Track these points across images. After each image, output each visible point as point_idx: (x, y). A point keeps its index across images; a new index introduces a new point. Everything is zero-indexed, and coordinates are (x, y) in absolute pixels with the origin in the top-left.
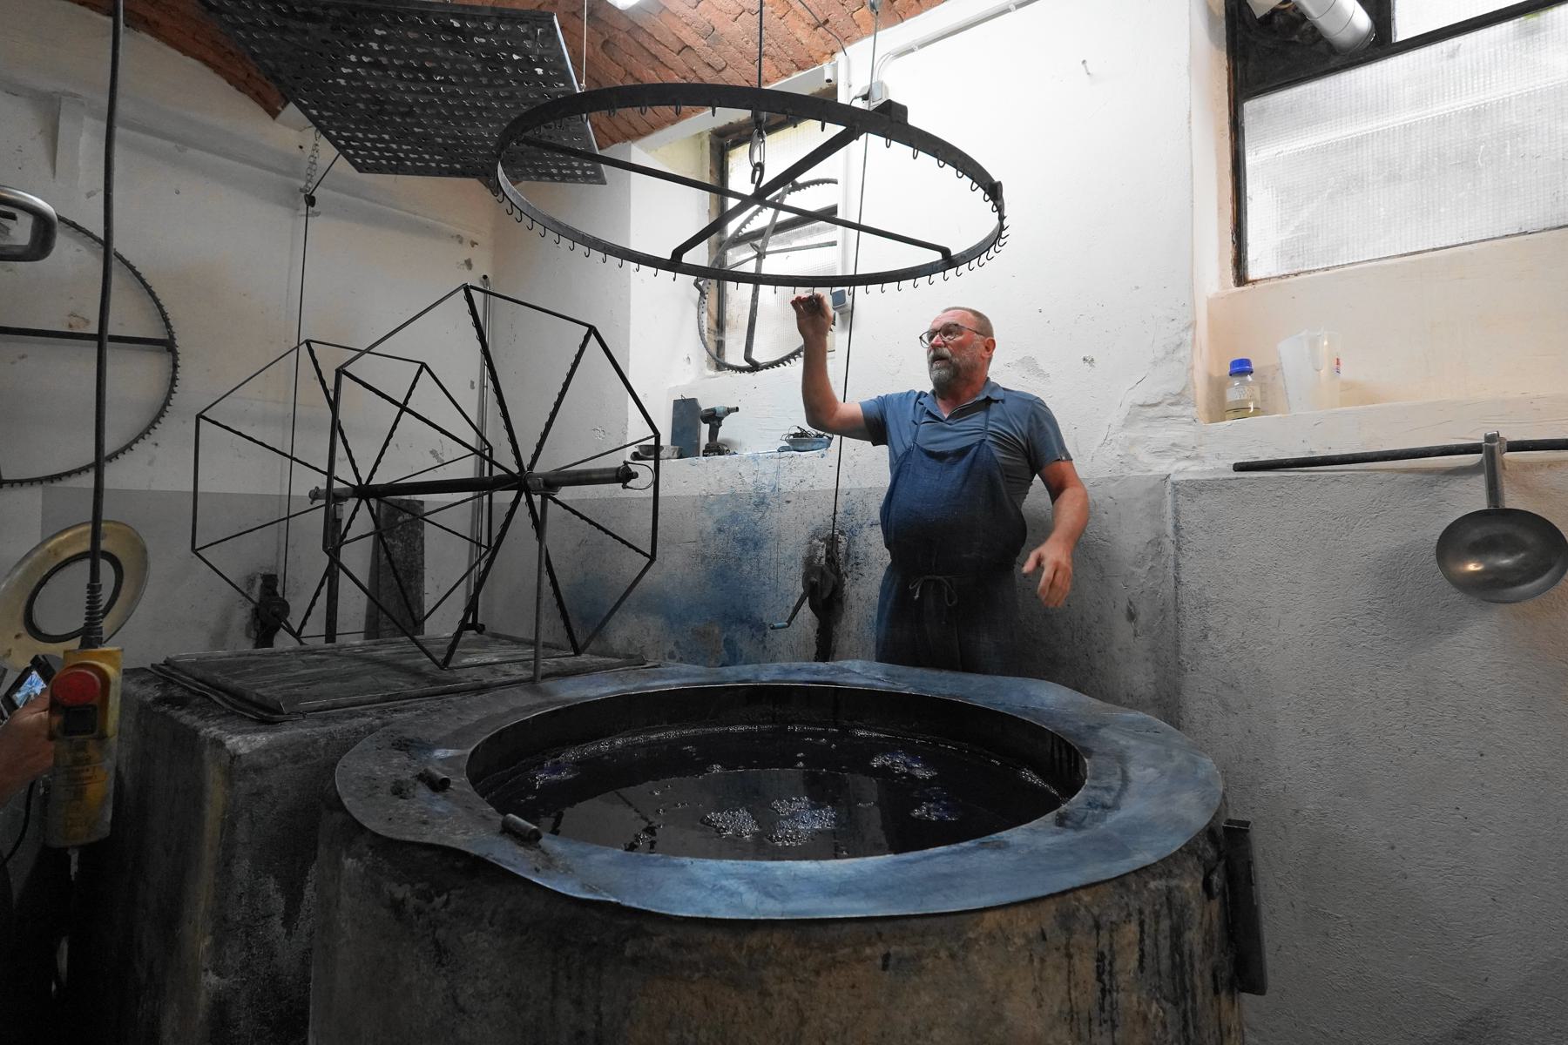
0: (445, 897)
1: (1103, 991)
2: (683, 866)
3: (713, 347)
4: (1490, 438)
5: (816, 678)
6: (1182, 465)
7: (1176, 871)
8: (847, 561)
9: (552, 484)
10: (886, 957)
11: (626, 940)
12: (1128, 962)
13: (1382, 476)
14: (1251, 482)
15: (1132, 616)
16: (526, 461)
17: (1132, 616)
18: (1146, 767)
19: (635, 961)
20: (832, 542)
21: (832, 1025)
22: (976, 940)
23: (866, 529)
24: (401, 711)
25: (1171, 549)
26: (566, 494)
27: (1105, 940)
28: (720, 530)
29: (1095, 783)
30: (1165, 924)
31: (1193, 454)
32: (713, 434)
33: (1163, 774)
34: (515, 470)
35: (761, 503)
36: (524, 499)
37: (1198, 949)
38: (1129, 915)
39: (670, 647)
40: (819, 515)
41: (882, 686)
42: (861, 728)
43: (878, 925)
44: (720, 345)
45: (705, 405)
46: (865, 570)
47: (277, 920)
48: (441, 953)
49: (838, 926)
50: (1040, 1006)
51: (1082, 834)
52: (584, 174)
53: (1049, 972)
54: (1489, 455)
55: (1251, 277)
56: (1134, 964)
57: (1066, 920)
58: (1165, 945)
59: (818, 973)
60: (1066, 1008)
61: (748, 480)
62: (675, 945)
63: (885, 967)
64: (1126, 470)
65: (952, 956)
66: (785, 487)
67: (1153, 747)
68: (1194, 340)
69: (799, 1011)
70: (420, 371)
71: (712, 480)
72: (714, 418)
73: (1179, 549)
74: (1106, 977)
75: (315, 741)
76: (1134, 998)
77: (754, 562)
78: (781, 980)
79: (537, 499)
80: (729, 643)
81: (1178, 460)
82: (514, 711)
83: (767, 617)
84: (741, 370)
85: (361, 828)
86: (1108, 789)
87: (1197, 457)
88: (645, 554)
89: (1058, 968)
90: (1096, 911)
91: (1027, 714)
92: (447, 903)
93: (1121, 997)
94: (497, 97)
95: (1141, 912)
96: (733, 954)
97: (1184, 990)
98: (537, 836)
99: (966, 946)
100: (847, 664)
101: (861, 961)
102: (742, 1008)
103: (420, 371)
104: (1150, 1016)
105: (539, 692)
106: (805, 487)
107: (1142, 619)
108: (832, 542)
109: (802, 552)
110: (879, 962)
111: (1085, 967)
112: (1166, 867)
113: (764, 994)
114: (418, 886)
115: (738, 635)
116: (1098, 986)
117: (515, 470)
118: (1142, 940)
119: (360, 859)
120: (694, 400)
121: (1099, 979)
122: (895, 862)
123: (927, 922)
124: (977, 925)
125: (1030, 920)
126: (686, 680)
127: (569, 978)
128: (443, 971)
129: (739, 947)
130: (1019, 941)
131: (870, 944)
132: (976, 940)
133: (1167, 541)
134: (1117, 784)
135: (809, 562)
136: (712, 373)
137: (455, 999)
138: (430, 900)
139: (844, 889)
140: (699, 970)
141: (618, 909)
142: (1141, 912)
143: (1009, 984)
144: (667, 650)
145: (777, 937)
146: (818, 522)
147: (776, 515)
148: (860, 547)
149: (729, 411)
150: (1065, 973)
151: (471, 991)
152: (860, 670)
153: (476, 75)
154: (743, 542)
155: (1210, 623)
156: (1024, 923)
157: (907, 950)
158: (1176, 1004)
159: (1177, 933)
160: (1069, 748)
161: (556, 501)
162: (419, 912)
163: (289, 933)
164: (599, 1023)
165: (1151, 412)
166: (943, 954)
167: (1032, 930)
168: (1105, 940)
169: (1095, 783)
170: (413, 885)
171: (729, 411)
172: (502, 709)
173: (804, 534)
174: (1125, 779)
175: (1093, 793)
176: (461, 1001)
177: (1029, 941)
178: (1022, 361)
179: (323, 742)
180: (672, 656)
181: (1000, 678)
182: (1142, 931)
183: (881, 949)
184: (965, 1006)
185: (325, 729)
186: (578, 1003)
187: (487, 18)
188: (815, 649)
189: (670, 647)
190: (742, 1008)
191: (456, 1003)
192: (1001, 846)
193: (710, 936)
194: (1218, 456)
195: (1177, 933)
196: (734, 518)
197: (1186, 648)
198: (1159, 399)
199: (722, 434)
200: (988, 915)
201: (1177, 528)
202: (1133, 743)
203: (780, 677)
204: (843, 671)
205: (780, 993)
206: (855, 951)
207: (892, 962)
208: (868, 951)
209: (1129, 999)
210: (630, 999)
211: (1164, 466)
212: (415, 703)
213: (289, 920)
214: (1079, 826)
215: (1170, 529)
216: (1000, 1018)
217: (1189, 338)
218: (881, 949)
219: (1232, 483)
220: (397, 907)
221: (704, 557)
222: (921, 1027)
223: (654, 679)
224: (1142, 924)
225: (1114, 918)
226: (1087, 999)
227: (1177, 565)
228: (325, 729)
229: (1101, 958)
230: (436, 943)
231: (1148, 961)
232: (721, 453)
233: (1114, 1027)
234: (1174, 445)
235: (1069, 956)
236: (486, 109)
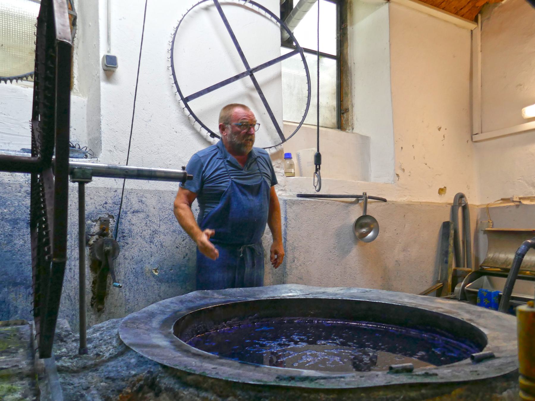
4: (365, 194)
13: (338, 203)
14: (308, 202)
23: (130, 215)
31: (283, 189)
46: (130, 240)
54: (362, 199)
55: (188, 103)
155: (295, 255)
194: (290, 191)
219: (302, 202)
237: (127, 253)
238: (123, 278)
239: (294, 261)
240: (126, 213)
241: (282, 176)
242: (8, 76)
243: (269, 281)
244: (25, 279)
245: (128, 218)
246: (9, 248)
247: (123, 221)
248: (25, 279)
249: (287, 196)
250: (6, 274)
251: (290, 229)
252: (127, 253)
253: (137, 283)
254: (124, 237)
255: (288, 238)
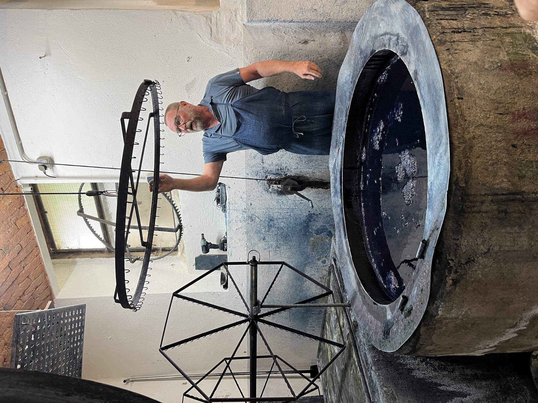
0: (450, 261)
1: (464, 31)
2: (431, 183)
3: (165, 253)
5: (338, 179)
6: (239, 18)
7: (422, 9)
8: (280, 175)
9: (256, 304)
10: (459, 98)
11: (460, 186)
12: (455, 24)
15: (306, 42)
16: (243, 318)
17: (306, 42)
18: (379, 27)
19: (466, 182)
20: (271, 182)
21: (482, 115)
22: (451, 70)
23: (265, 165)
24: (367, 361)
25: (277, 24)
26: (260, 298)
27: (448, 31)
28: (264, 239)
29: (387, 46)
30: (441, 12)
31: (234, 13)
32: (215, 247)
33: (382, 20)
34: (248, 323)
35: (251, 218)
36: (262, 318)
37: (448, 3)
38: (439, 23)
39: (320, 263)
40: (259, 188)
41: (341, 148)
42: (361, 156)
43: (448, 102)
44: (164, 250)
45: (200, 252)
46: (284, 165)
47: (464, 400)
48: (470, 261)
49: (450, 115)
50: (471, 51)
51: (410, 45)
52: (81, 315)
53: (459, 47)
56: (455, 22)
57: (442, 43)
58: (447, 13)
59: (466, 120)
60: (471, 43)
61: (240, 225)
62: (460, 169)
63: (462, 99)
64: (240, 43)
65: (457, 77)
66: (243, 205)
67: (370, 26)
68: (181, 11)
69: (479, 126)
70: (188, 396)
71: (239, 244)
72: (207, 247)
73: (277, 20)
74: (460, 30)
75: (385, 392)
76: (466, 22)
77: (279, 221)
78: (469, 132)
79: (263, 311)
80: (318, 232)
81: (236, 20)
82: (365, 302)
83: (305, 214)
84: (181, 234)
85: (426, 312)
86: (390, 39)
87: (235, 12)
88: (281, 267)
89: (458, 45)
90: (438, 34)
91: (354, 81)
92: (452, 260)
93: (466, 26)
94: (48, 353)
95: (437, 19)
96: (461, 148)
97: (462, 7)
98: (424, 241)
99: (453, 73)
100: (331, 166)
101: (461, 107)
102: (479, 145)
103: (188, 396)
104: (471, 17)
105: (354, 298)
106: (244, 196)
107: (307, 38)
108: (270, 181)
109: (275, 196)
110: (460, 100)
111: (457, 37)
112: (421, 13)
113: (474, 138)
114: (447, 274)
115: (314, 228)
116: (463, 33)
117: (248, 323)
118: (447, 19)
119: (438, 307)
120: (196, 258)
121: (460, 32)
122: (425, 107)
123: (446, 86)
124: (446, 70)
125: (443, 54)
126: (343, 236)
127: (474, 207)
128: (476, 259)
129: (459, 147)
130: (450, 57)
131: (455, 104)
132: (451, 70)
133: (272, 27)
134: (387, 37)
135: (281, 193)
136: (179, 253)
137: (485, 253)
138: (452, 267)
139: (436, 120)
140: (468, 160)
141: (449, 192)
142: (437, 19)
143: (464, 60)
144: (322, 265)
145: (455, 135)
146: (261, 189)
147: (257, 210)
148: (273, 168)
149: (203, 238)
150: (459, 43)
151: (482, 246)
152: (335, 159)
153: (39, 362)
154: (270, 226)
155: (309, 8)
156: (444, 55)
157: (456, 92)
158: (466, 10)
159: (443, 9)
160: (370, 60)
161: (263, 301)
162: (456, 272)
163: (469, 395)
164: (488, 195)
165: (214, 30)
166: (456, 80)
167: (446, 53)
168: (448, 31)
169: (387, 46)
170: (447, 276)
171: (203, 238)
172: (365, 308)
173: (267, 196)
174: (386, 34)
175: (392, 45)
176: (486, 250)
177: (450, 54)
178: (187, 91)
179: (385, 389)
180: (324, 262)
181: (337, 96)
182: (444, 19)
183: (456, 100)
184: (473, 73)
185: (379, 389)
186: (482, 202)
187: (17, 349)
188: (320, 189)
189: (320, 263)
190: (479, 145)
191: (486, 252)
192: (416, 73)
193: (456, 157)
195: (443, 9)
196: (258, 232)
197: (320, 18)
198: (209, 28)
199: (214, 242)
200: (442, 67)
201: (268, 21)
202: (368, 34)
203: (339, 195)
204: (334, 167)
205: (473, 132)
206: (457, 108)
207: (460, 96)
208: (457, 104)
209: (467, 24)
210: (479, 184)
211: (239, 27)
212: (362, 358)
213: (464, 395)
214: (407, 46)
215: (268, 24)
216: (476, 63)
217: (180, 13)
218: (456, 100)
220: (455, 282)
221: (277, 247)
222: (480, 87)
223: (343, 251)
224: (441, 19)
225: (440, 28)
226: (468, 36)
227: (284, 21)
228: (379, 389)
229: (454, 32)
230: (467, 263)
231: (453, 18)
232: (225, 241)
233: (475, 28)
234: (230, 22)
235: (454, 42)
236: (53, 361)
237: (293, 167)
238: (311, 170)
239: (315, 10)
240: (264, 168)
241: (220, 14)
242: (171, 206)
243: (333, 37)
244: (305, 222)
245: (267, 166)
246: (286, 229)
247: (269, 170)
248: (305, 222)
249: (242, 9)
250: (301, 230)
251: (279, 15)
252: (293, 167)
253: (316, 160)
254: (281, 169)
255: (290, 19)
